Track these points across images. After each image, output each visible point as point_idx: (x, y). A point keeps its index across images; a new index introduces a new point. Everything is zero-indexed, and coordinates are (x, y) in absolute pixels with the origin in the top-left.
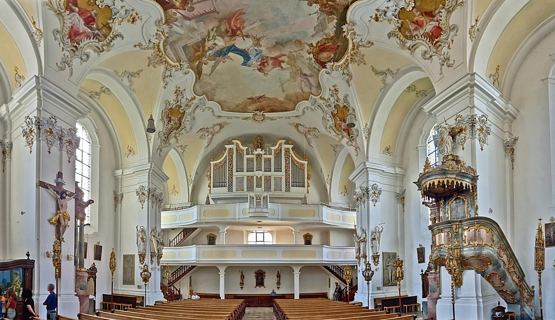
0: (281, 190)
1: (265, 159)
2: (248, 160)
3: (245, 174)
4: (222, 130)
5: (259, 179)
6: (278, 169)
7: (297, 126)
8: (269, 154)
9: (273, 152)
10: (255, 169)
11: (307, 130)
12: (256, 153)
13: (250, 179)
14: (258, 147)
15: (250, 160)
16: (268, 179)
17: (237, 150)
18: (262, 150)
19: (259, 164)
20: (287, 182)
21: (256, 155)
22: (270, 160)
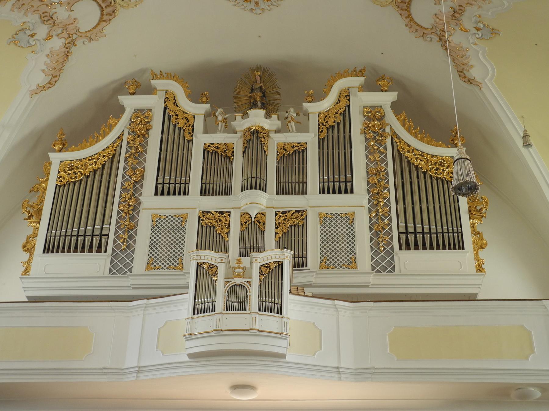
0: (352, 264)
1: (282, 148)
2: (210, 152)
4: (109, 29)
8: (299, 130)
12: (242, 124)
14: (254, 106)
15: (217, 156)
18: (268, 116)
20: (378, 232)
22: (300, 152)
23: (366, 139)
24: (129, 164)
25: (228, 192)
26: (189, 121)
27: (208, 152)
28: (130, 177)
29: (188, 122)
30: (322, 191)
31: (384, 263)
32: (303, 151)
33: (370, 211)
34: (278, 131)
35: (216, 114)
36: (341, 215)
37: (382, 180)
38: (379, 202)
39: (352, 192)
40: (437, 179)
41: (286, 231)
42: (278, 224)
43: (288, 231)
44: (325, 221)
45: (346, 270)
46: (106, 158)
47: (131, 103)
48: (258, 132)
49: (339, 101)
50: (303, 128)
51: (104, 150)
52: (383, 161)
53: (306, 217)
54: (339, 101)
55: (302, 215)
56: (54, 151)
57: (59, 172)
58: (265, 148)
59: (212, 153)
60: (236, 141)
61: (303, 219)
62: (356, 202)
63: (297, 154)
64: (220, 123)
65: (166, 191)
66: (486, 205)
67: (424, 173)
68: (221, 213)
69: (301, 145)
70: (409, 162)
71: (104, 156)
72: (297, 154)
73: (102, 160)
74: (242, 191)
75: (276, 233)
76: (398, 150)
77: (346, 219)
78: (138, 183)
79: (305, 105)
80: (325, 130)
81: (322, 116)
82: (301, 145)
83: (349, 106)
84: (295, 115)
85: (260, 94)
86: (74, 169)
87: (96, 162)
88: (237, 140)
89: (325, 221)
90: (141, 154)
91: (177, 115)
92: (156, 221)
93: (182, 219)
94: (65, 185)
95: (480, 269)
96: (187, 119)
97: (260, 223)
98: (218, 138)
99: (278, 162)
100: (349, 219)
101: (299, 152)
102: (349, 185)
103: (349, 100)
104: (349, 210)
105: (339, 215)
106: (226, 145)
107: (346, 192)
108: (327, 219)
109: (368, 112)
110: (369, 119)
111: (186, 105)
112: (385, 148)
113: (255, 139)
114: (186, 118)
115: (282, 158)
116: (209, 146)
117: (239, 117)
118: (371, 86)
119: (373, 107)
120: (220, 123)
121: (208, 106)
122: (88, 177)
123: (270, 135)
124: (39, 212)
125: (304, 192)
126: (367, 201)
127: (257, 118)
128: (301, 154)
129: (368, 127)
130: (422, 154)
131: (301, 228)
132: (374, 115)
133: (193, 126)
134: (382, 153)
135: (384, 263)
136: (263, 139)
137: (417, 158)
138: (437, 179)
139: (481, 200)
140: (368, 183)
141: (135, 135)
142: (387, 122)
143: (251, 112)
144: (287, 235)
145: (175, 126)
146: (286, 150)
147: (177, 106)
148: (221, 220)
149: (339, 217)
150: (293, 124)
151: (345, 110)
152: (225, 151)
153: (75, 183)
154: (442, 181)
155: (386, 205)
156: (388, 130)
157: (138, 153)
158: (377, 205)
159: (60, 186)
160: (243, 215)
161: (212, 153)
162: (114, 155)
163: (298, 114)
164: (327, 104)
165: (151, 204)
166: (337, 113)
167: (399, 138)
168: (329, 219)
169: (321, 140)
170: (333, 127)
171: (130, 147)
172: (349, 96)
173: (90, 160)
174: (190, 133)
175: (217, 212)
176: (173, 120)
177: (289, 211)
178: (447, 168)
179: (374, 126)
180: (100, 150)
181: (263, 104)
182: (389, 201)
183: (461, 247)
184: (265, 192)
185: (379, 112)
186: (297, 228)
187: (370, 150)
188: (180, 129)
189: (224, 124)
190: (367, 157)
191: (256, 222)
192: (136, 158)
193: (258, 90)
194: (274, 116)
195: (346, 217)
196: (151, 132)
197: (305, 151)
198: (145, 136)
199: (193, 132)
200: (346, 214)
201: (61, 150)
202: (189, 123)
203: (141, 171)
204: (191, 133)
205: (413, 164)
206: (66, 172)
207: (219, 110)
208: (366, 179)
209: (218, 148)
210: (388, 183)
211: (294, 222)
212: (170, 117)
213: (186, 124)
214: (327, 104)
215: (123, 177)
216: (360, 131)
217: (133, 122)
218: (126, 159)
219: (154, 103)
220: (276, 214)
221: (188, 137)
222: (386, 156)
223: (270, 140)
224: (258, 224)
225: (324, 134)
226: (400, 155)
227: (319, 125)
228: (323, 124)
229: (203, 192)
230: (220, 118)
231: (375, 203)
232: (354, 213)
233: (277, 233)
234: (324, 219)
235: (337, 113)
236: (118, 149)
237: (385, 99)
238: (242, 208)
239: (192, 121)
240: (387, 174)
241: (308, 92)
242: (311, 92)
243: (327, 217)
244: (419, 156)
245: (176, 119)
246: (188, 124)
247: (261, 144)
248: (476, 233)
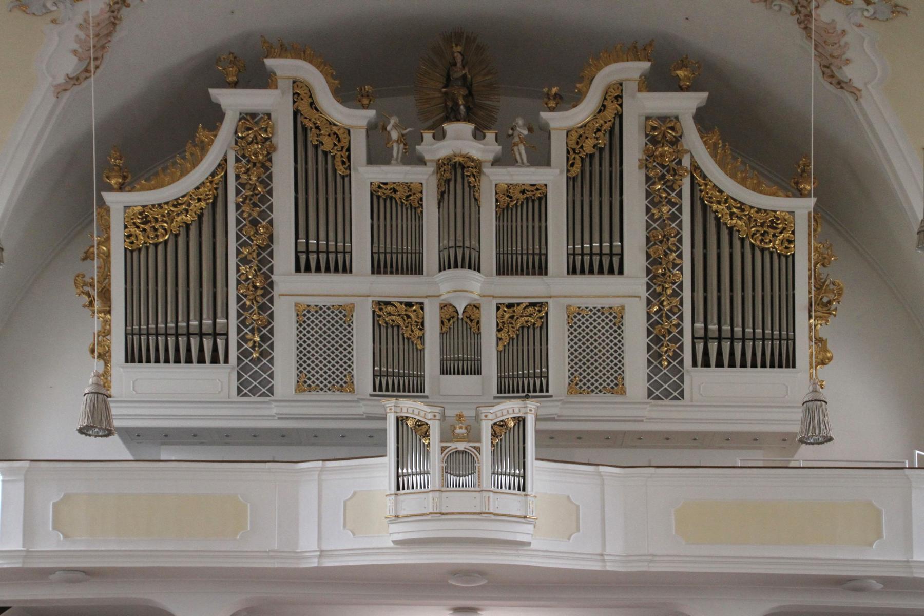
2: (382, 197)
3: (360, 288)
5: (461, 324)
9: (558, 149)
10: (431, 257)
12: (435, 150)
13: (396, 326)
14: (452, 115)
16: (525, 328)
17: (301, 131)
18: (478, 135)
22: (536, 199)
23: (648, 178)
24: (245, 215)
25: (416, 269)
26: (341, 136)
27: (379, 197)
28: (249, 238)
29: (339, 141)
30: (572, 271)
32: (540, 199)
33: (649, 303)
34: (496, 162)
35: (389, 128)
36: (601, 310)
37: (672, 251)
38: (664, 289)
39: (621, 272)
40: (763, 250)
41: (515, 336)
42: (500, 325)
43: (518, 336)
44: (576, 320)
46: (203, 204)
48: (463, 167)
49: (604, 106)
50: (541, 158)
51: (197, 188)
52: (674, 217)
53: (547, 313)
54: (604, 106)
55: (540, 311)
56: (110, 189)
57: (126, 227)
58: (477, 194)
59: (385, 200)
60: (423, 177)
61: (541, 318)
62: (627, 291)
63: (530, 204)
64: (395, 145)
65: (313, 265)
66: (840, 294)
67: (742, 240)
68: (409, 305)
69: (537, 189)
70: (718, 220)
71: (199, 200)
72: (530, 204)
73: (196, 206)
74: (440, 271)
75: (499, 339)
76: (702, 200)
77: (611, 317)
79: (545, 115)
80: (578, 162)
81: (574, 136)
82: (537, 189)
83: (621, 117)
84: (526, 132)
85: (464, 92)
86: (150, 222)
87: (187, 211)
88: (426, 177)
89: (576, 320)
90: (264, 199)
91: (317, 128)
94: (139, 250)
96: (338, 136)
97: (471, 321)
98: (395, 174)
99: (498, 219)
100: (615, 317)
101: (533, 201)
102: (616, 260)
103: (621, 105)
104: (615, 303)
105: (599, 310)
106: (408, 185)
107: (611, 271)
108: (579, 317)
109: (654, 129)
110: (654, 141)
112: (680, 195)
113: (458, 174)
114: (335, 133)
115: (503, 211)
116: (379, 187)
117: (428, 136)
119: (663, 119)
120: (395, 145)
121: (371, 113)
122: (176, 236)
123: (485, 170)
125: (541, 269)
126: (645, 287)
127: (459, 139)
128: (537, 204)
129: (650, 155)
130: (742, 206)
131: (537, 331)
132: (662, 133)
133: (349, 150)
134: (673, 205)
136: (472, 179)
137: (732, 214)
138: (763, 250)
139: (831, 287)
140: (648, 256)
141: (249, 161)
142: (685, 147)
143: (450, 128)
144: (515, 341)
145: (316, 147)
146: (511, 197)
147: (317, 110)
148: (409, 317)
149: (599, 314)
150: (522, 148)
151: (614, 124)
152: (407, 197)
153: (156, 245)
154: (771, 253)
155: (675, 294)
156: (686, 162)
157: (258, 199)
158: (660, 294)
159: (132, 251)
160: (443, 307)
161: (385, 200)
162: (215, 198)
163: (530, 130)
164: (581, 114)
166: (599, 130)
167: (705, 177)
168: (583, 317)
169: (571, 180)
170: (591, 156)
171: (243, 185)
172: (621, 97)
173: (175, 206)
174: (343, 163)
175: (401, 303)
176: (312, 138)
177: (519, 304)
178: (781, 233)
179: (662, 155)
180: (191, 189)
181: (468, 109)
182: (681, 286)
184: (479, 271)
185: (672, 129)
186: (531, 330)
187: (653, 200)
188: (326, 154)
189: (402, 146)
190: (648, 210)
191: (465, 319)
192: (255, 205)
193: (460, 83)
194: (490, 136)
195: (611, 314)
196: (275, 157)
197: (543, 199)
198: (266, 166)
199: (349, 161)
200: (611, 308)
201: (121, 188)
202: (342, 144)
203: (267, 229)
204: (347, 162)
205: (726, 224)
206: (138, 227)
207: (393, 120)
208: (644, 248)
209: (395, 191)
210: (680, 256)
211: (527, 322)
212: (305, 129)
213: (335, 145)
214: (581, 114)
215: (238, 238)
216: (637, 163)
217: (242, 138)
218: (238, 207)
220: (498, 309)
221: (341, 170)
222: (680, 210)
223: (483, 178)
224: (469, 322)
225: (576, 170)
226: (705, 208)
227: (568, 152)
228: (574, 150)
229: (377, 269)
230: (395, 135)
231: (659, 289)
232: (623, 308)
233: (501, 339)
234: (575, 317)
235: (599, 130)
236: (221, 186)
237: (684, 104)
238: (443, 297)
239: (346, 140)
240: (680, 241)
241: (550, 90)
242: (555, 90)
243: (579, 314)
244: (735, 210)
245: (318, 136)
246: (339, 145)
247: (469, 186)
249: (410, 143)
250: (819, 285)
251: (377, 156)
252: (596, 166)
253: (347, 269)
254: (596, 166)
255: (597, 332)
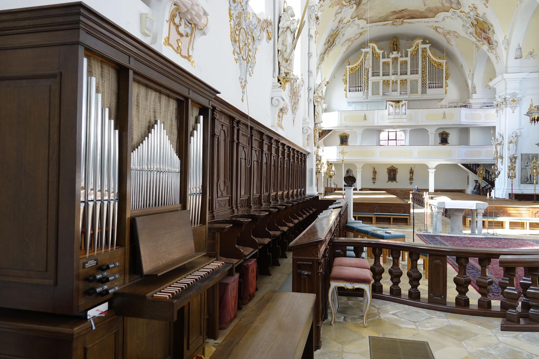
0: (417, 92)
2: (384, 63)
3: (380, 79)
6: (414, 72)
7: (436, 28)
10: (391, 74)
11: (446, 32)
12: (392, 56)
17: (373, 54)
19: (395, 67)
21: (392, 58)
22: (406, 62)
31: (424, 92)
34: (401, 57)
45: (416, 94)
47: (364, 50)
50: (406, 56)
60: (390, 60)
62: (418, 77)
78: (368, 73)
92: (373, 83)
93: (378, 83)
95: (446, 93)
98: (386, 60)
111: (378, 51)
113: (396, 59)
115: (401, 65)
118: (424, 43)
124: (346, 81)
125: (406, 74)
127: (395, 54)
135: (424, 92)
143: (394, 52)
165: (372, 79)
183: (442, 87)
219: (369, 50)
237: (427, 46)
248: (446, 83)
249: (388, 55)
250: (447, 74)
251: (384, 57)
252: (414, 56)
253: (379, 75)
254: (414, 56)
255: (414, 83)
